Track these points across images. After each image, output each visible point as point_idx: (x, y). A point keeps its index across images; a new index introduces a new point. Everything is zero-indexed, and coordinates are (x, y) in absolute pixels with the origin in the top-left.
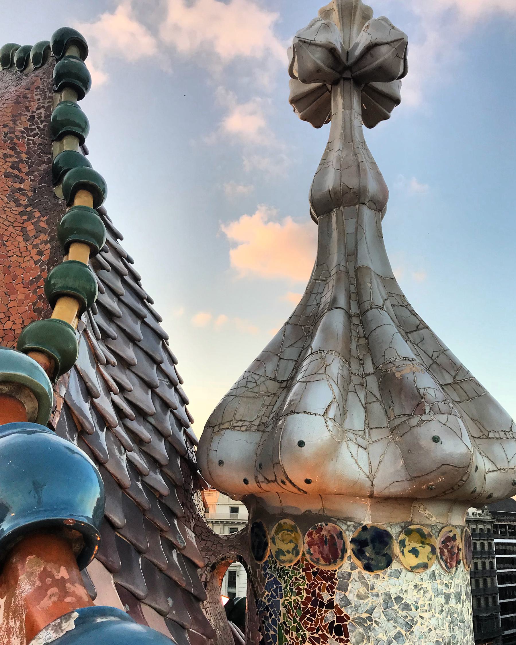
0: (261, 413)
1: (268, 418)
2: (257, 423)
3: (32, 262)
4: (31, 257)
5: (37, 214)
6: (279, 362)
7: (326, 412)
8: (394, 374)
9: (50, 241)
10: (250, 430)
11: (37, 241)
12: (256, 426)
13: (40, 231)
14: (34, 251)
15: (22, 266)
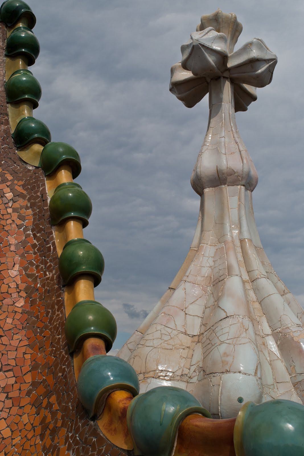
0: (182, 365)
1: (189, 369)
2: (179, 373)
3: (14, 226)
4: (13, 221)
5: (10, 177)
6: (185, 318)
7: (256, 373)
8: (293, 338)
9: (31, 207)
10: (174, 380)
11: (16, 205)
12: (179, 377)
13: (17, 195)
14: (15, 216)
15: (6, 228)
